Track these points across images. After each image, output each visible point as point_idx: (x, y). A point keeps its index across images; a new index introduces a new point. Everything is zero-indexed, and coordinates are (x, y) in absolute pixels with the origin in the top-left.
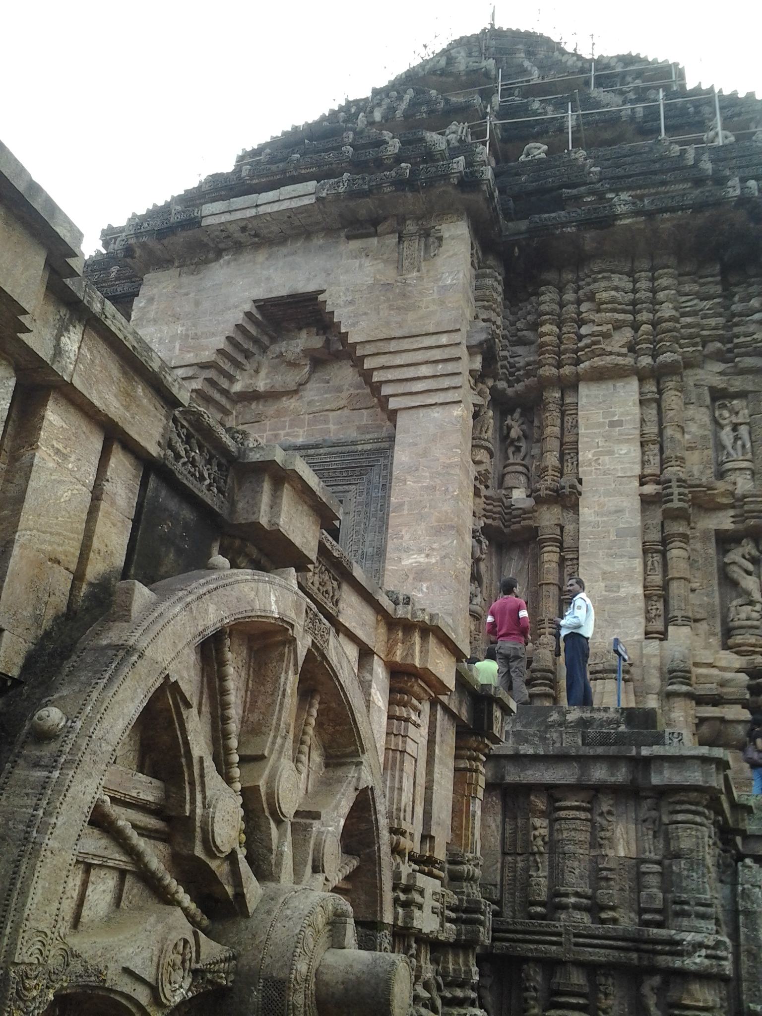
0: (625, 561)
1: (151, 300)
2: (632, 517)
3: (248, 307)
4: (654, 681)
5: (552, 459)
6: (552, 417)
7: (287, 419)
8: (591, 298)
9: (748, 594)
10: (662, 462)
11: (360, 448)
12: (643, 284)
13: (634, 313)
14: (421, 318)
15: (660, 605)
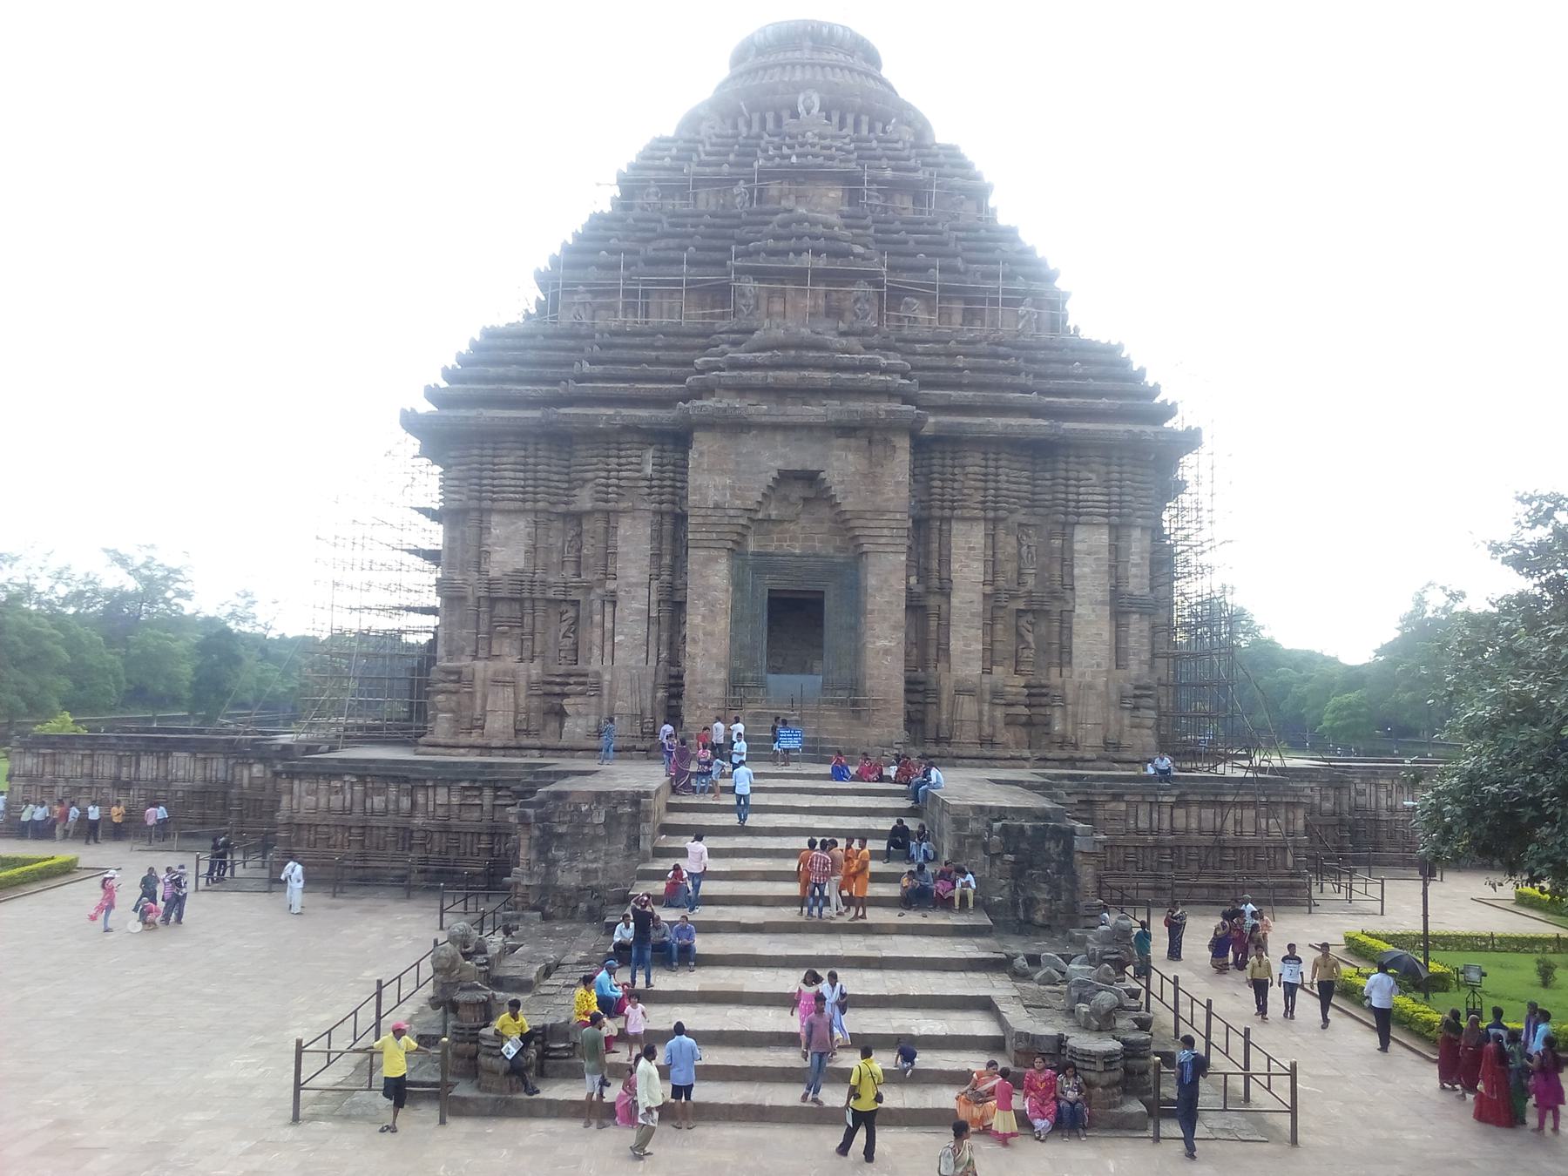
0: (973, 630)
1: (701, 454)
2: (978, 607)
3: (775, 474)
4: (987, 697)
5: (935, 565)
6: (935, 536)
7: (788, 535)
8: (963, 467)
9: (1028, 643)
10: (994, 573)
11: (835, 560)
12: (991, 463)
13: (986, 481)
14: (887, 500)
15: (988, 654)
